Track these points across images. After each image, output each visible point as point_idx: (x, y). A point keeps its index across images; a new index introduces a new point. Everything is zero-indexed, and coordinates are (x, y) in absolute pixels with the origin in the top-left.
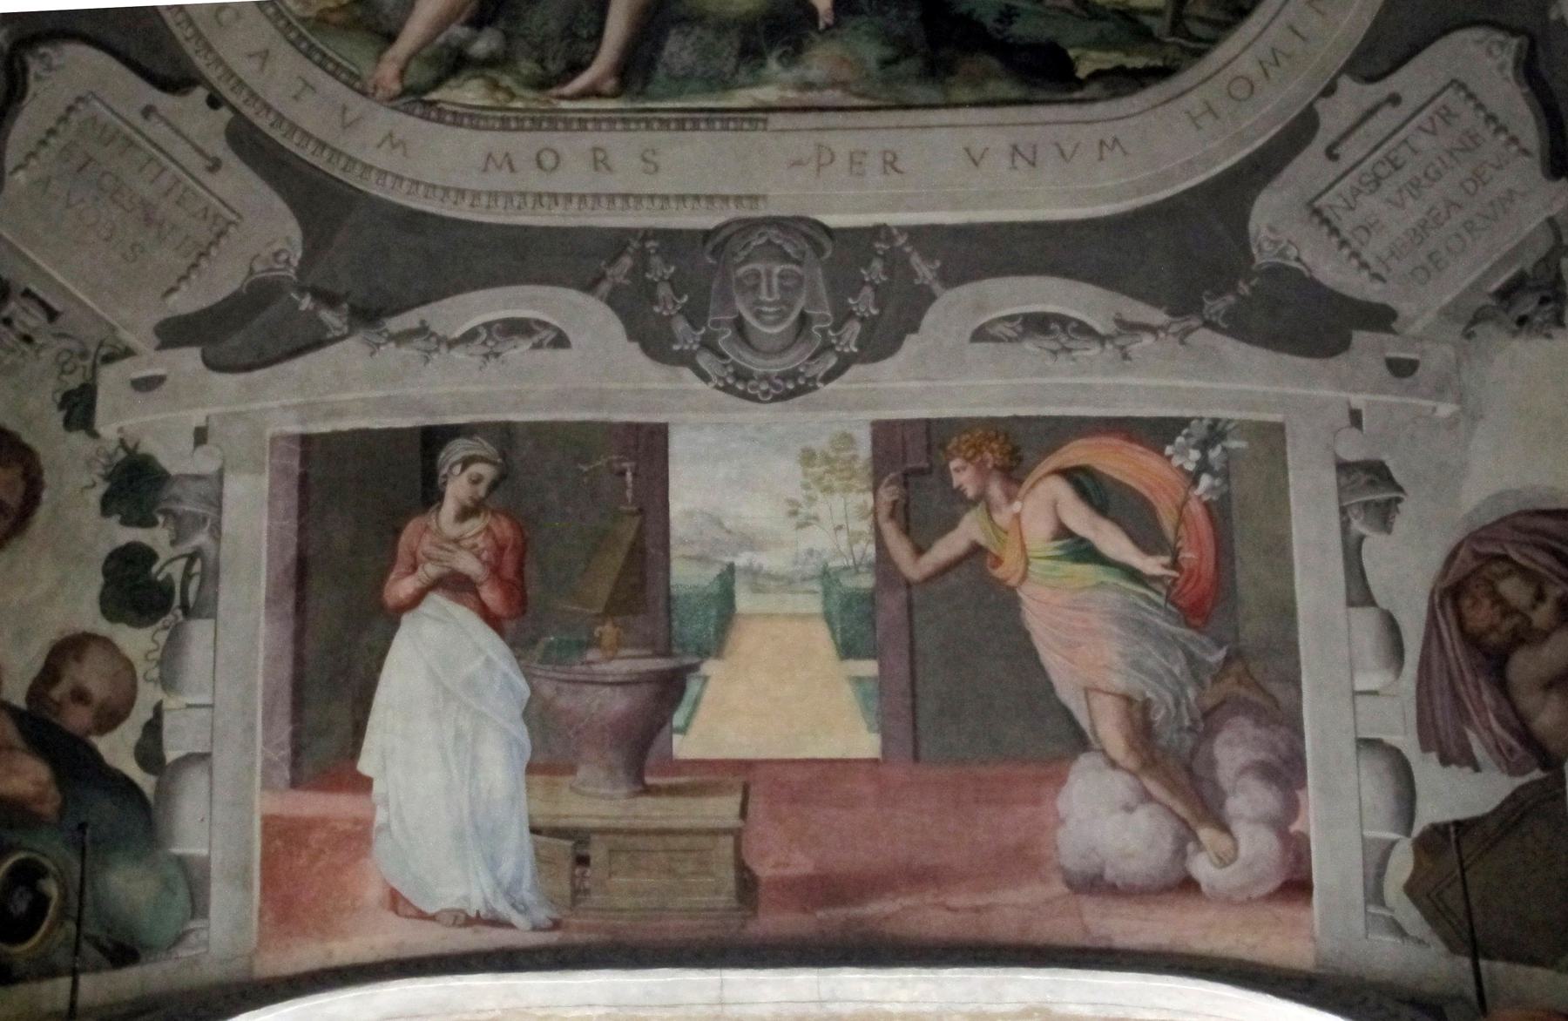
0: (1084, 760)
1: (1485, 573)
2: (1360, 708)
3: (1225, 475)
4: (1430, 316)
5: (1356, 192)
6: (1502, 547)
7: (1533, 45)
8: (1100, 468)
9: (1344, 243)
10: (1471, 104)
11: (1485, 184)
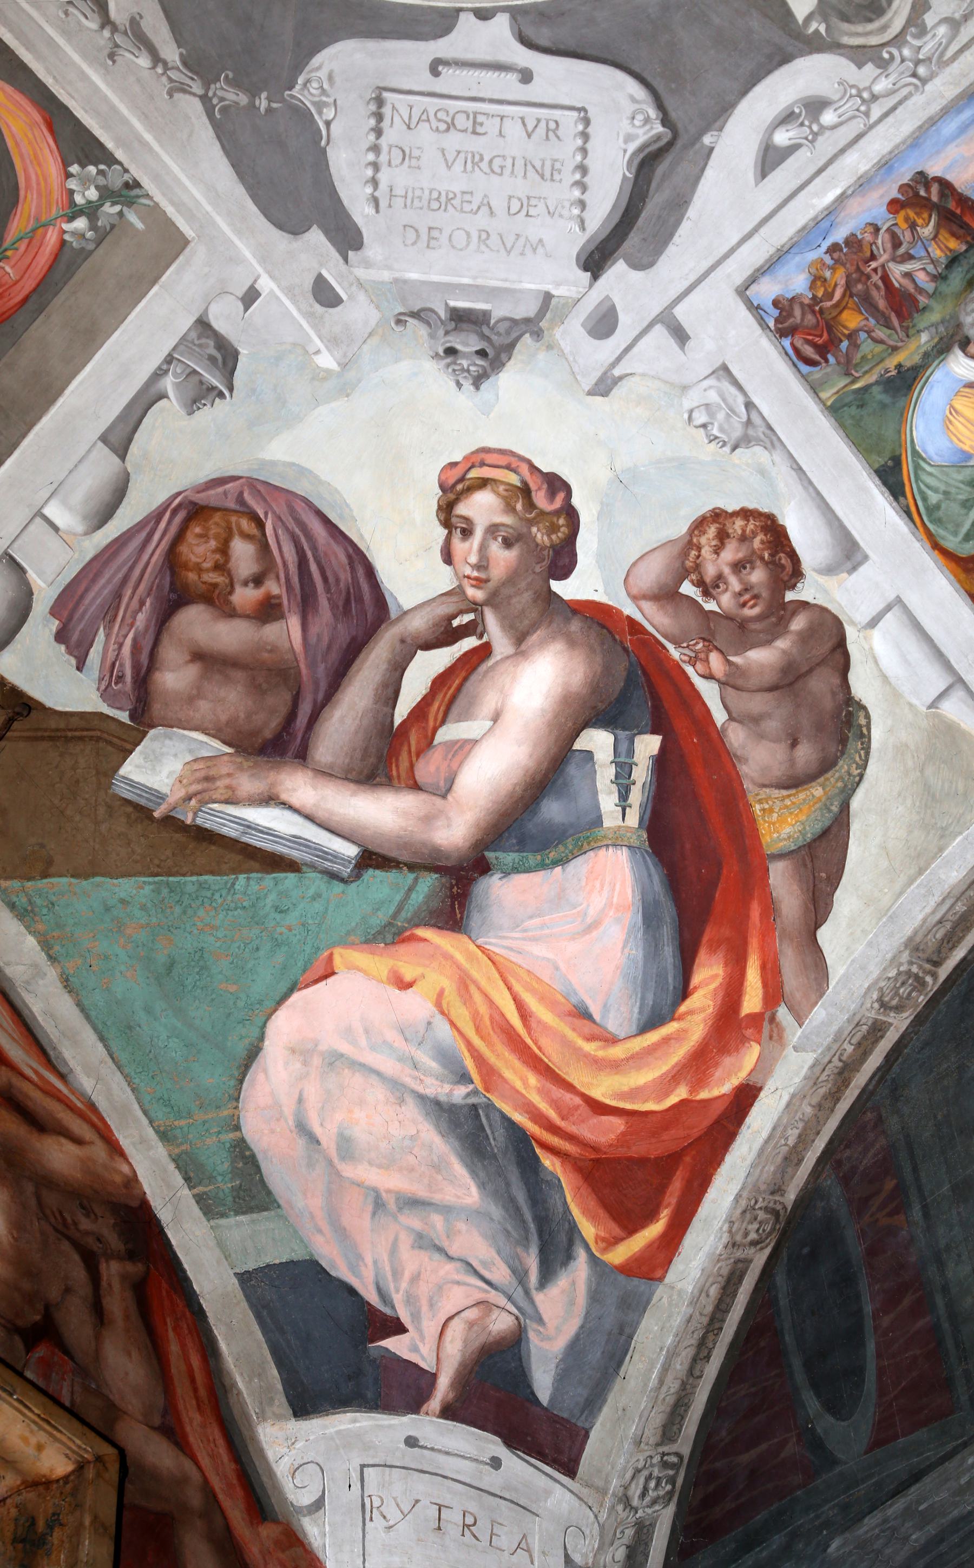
1: (233, 519)
2: (32, 528)
4: (386, 276)
5: (424, 117)
6: (266, 514)
7: (670, 145)
10: (579, 142)
11: (527, 215)
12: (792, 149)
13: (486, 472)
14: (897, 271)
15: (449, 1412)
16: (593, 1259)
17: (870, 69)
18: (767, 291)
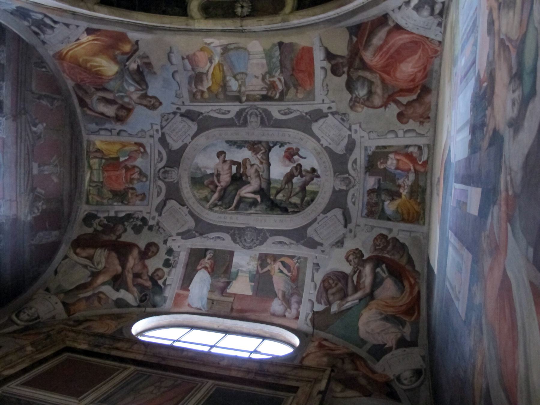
0: (276, 299)
3: (299, 263)
8: (285, 261)
9: (318, 235)
12: (355, 201)
13: (349, 254)
14: (373, 201)
15: (396, 349)
16: (409, 322)
17: (355, 187)
18: (364, 214)
